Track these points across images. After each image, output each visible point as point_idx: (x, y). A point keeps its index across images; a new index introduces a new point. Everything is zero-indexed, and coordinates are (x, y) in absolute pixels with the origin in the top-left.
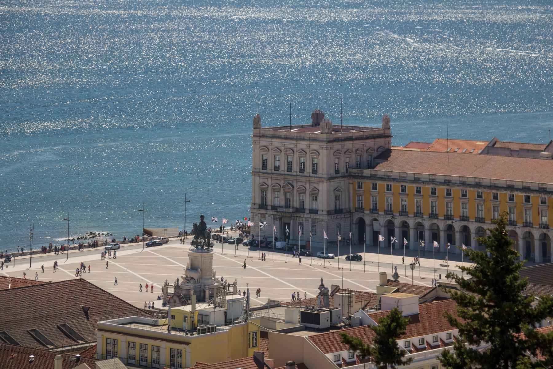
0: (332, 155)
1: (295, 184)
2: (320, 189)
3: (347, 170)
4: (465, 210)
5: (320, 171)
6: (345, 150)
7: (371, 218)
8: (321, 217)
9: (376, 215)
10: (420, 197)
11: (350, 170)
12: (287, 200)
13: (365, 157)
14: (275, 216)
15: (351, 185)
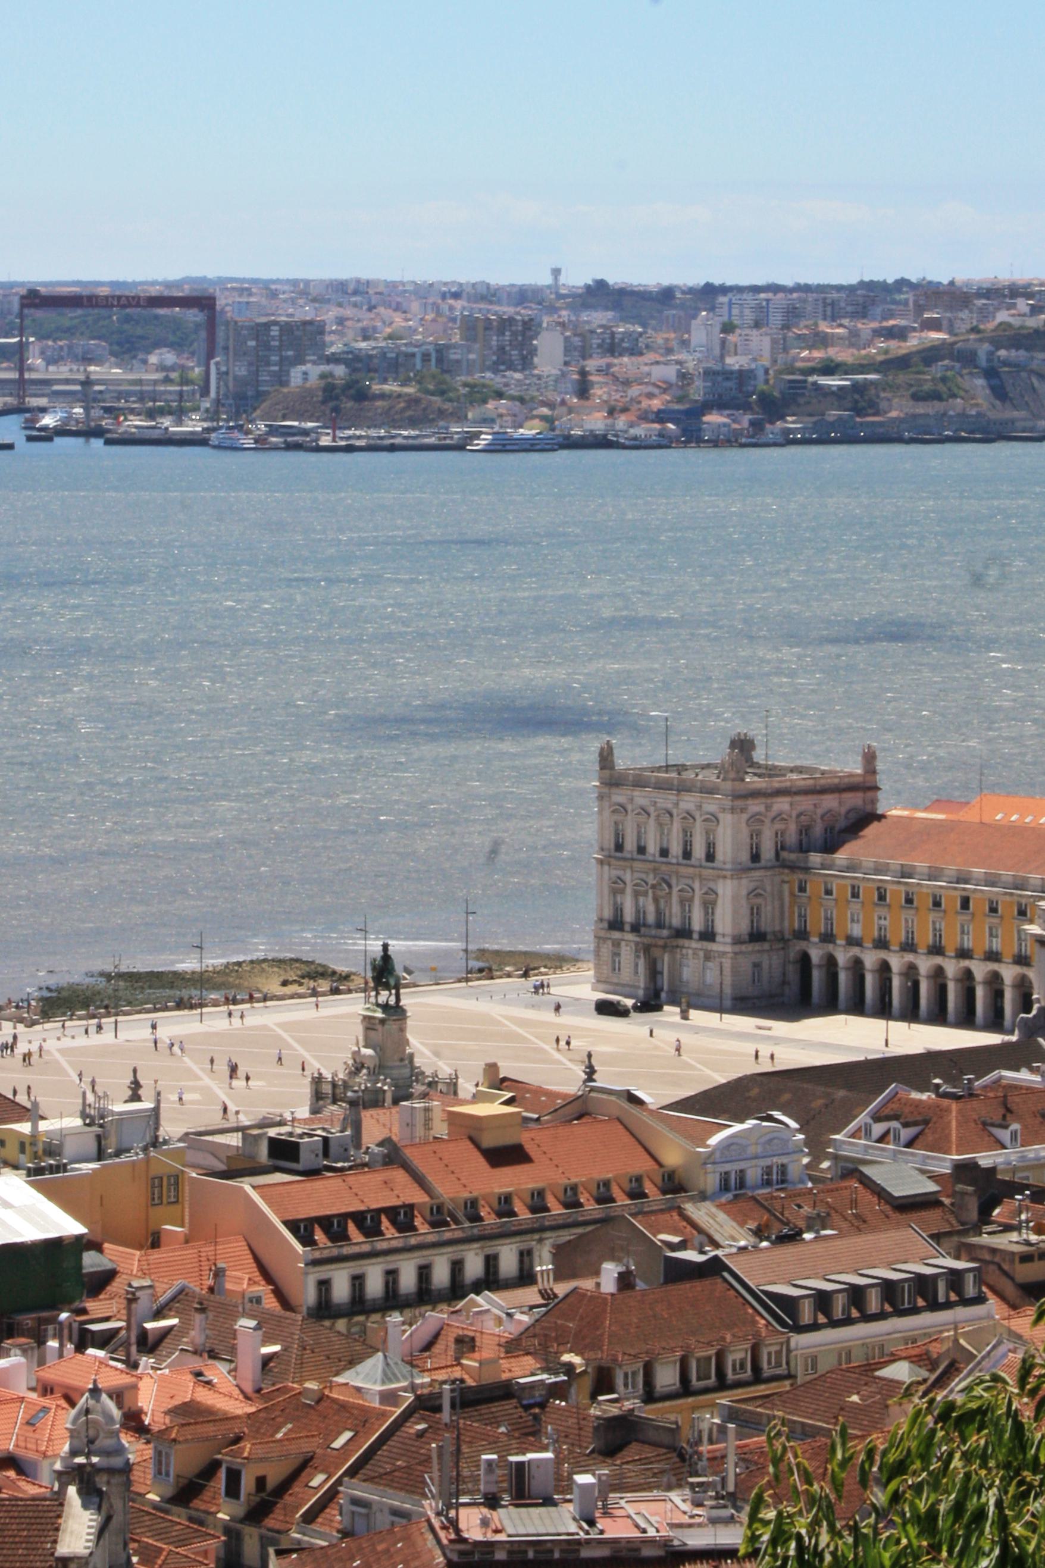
0: (744, 825)
1: (674, 882)
2: (720, 891)
3: (777, 855)
4: (994, 940)
5: (720, 856)
6: (773, 814)
7: (821, 952)
8: (721, 948)
9: (831, 946)
10: (913, 912)
11: (784, 854)
12: (659, 913)
13: (818, 830)
14: (637, 944)
15: (786, 887)
